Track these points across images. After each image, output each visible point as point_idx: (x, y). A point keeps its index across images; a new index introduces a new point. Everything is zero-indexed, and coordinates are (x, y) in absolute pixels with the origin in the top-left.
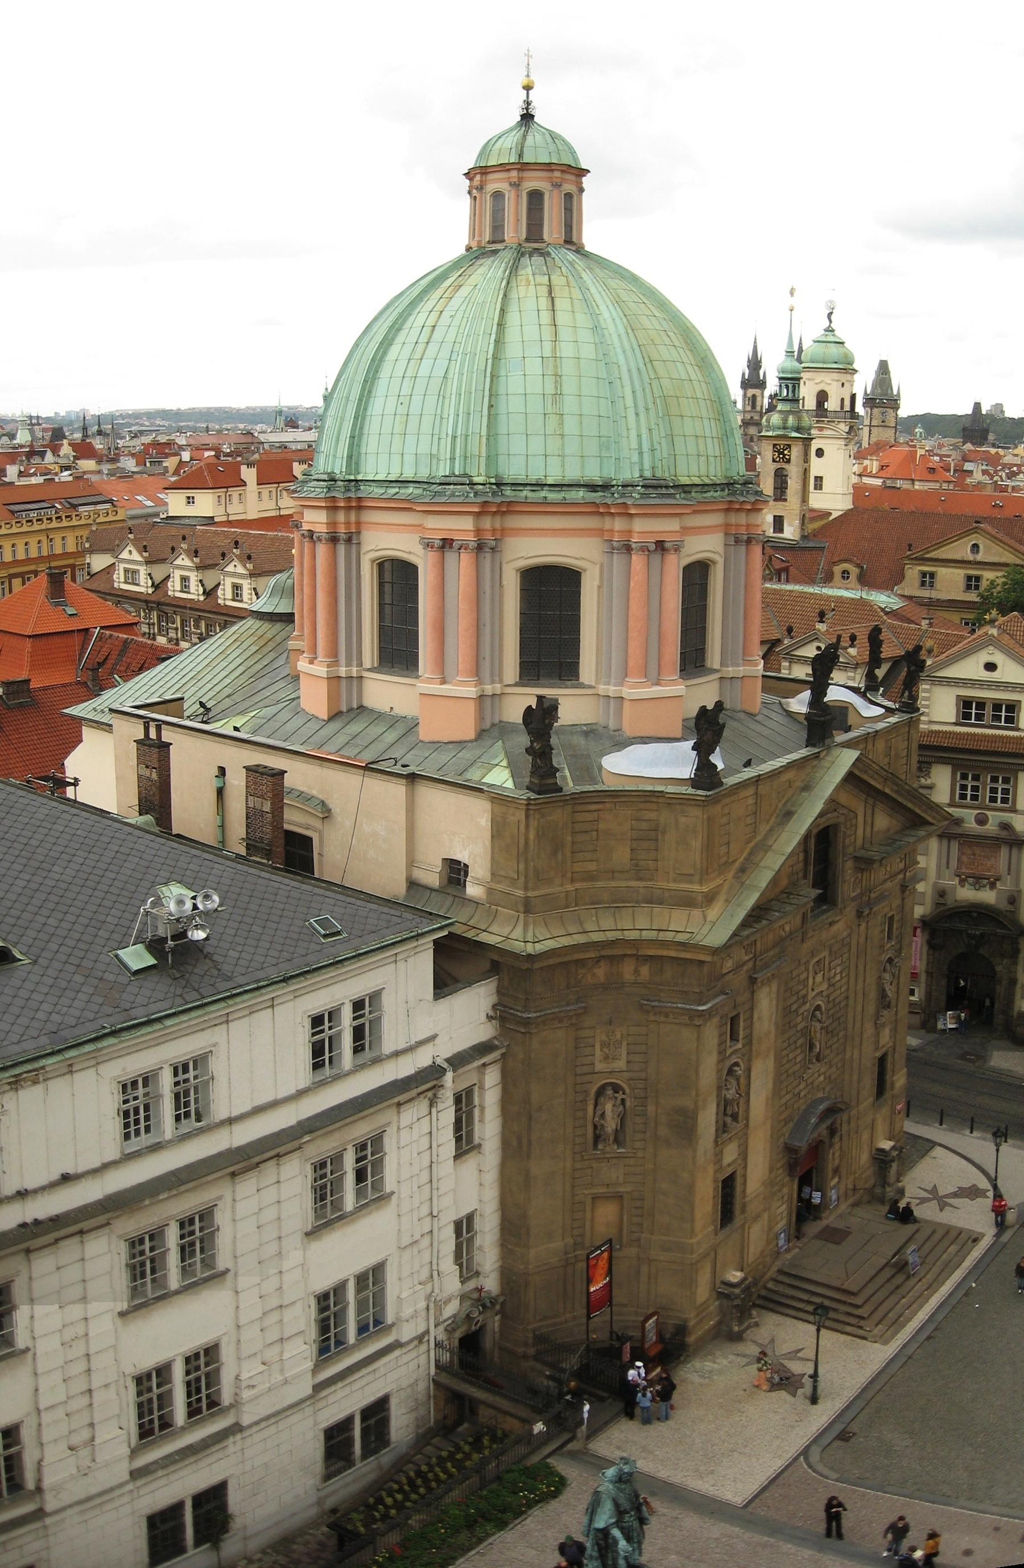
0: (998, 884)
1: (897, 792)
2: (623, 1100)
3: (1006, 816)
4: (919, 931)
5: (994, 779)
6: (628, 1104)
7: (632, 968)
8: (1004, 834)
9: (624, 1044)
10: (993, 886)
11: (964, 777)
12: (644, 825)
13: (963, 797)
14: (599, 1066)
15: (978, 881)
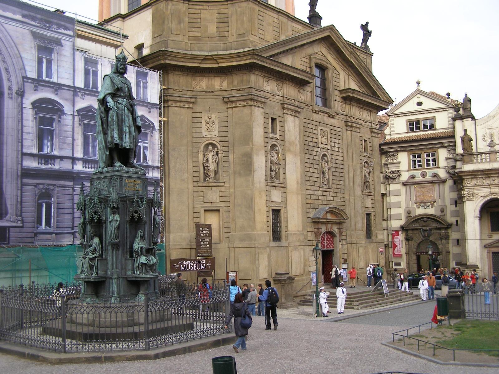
0: (435, 204)
1: (358, 65)
2: (217, 152)
3: (435, 171)
4: (400, 233)
5: (428, 155)
6: (220, 155)
7: (219, 82)
8: (435, 179)
9: (217, 122)
10: (433, 205)
11: (414, 157)
12: (222, 16)
13: (415, 166)
14: (205, 133)
15: (425, 204)
